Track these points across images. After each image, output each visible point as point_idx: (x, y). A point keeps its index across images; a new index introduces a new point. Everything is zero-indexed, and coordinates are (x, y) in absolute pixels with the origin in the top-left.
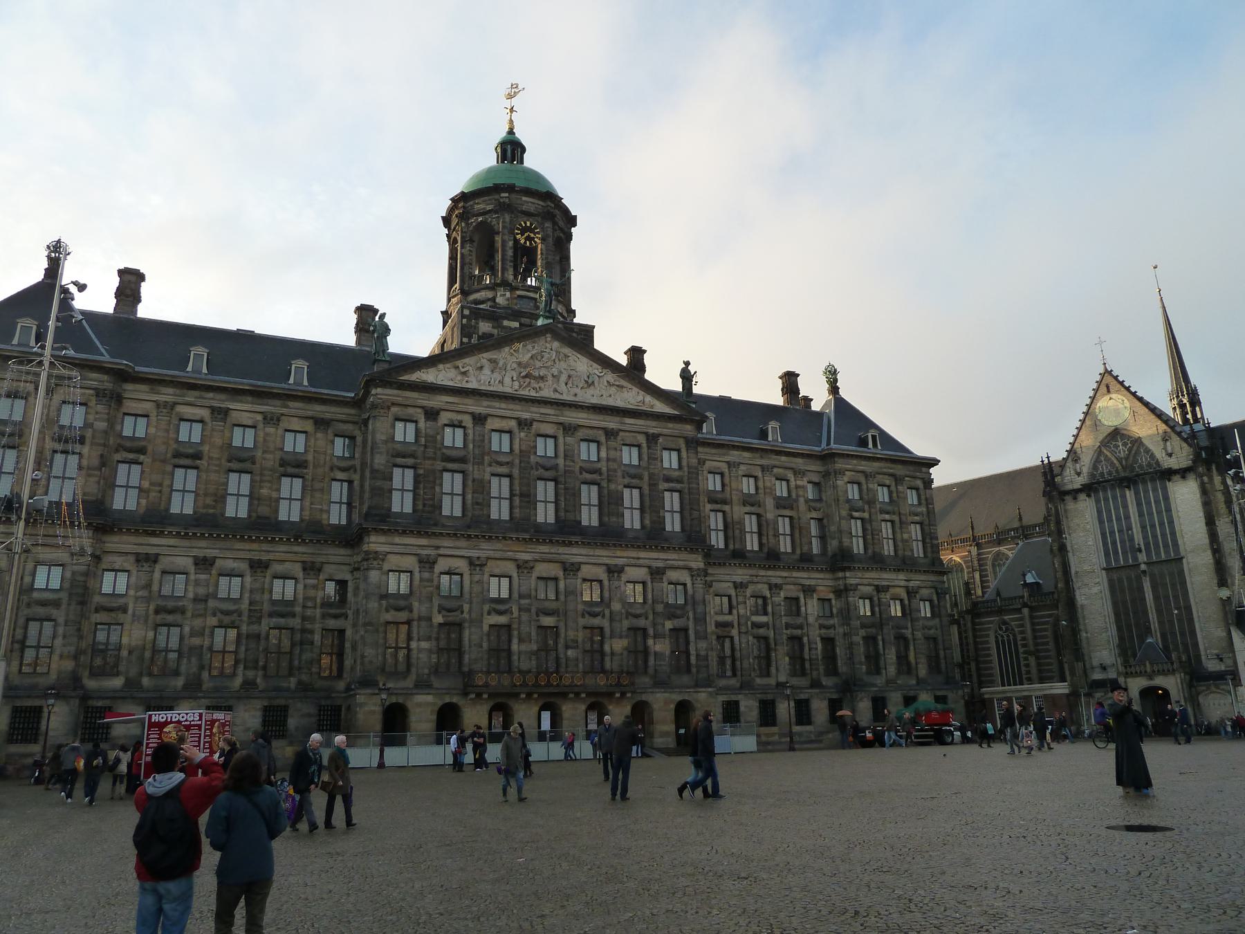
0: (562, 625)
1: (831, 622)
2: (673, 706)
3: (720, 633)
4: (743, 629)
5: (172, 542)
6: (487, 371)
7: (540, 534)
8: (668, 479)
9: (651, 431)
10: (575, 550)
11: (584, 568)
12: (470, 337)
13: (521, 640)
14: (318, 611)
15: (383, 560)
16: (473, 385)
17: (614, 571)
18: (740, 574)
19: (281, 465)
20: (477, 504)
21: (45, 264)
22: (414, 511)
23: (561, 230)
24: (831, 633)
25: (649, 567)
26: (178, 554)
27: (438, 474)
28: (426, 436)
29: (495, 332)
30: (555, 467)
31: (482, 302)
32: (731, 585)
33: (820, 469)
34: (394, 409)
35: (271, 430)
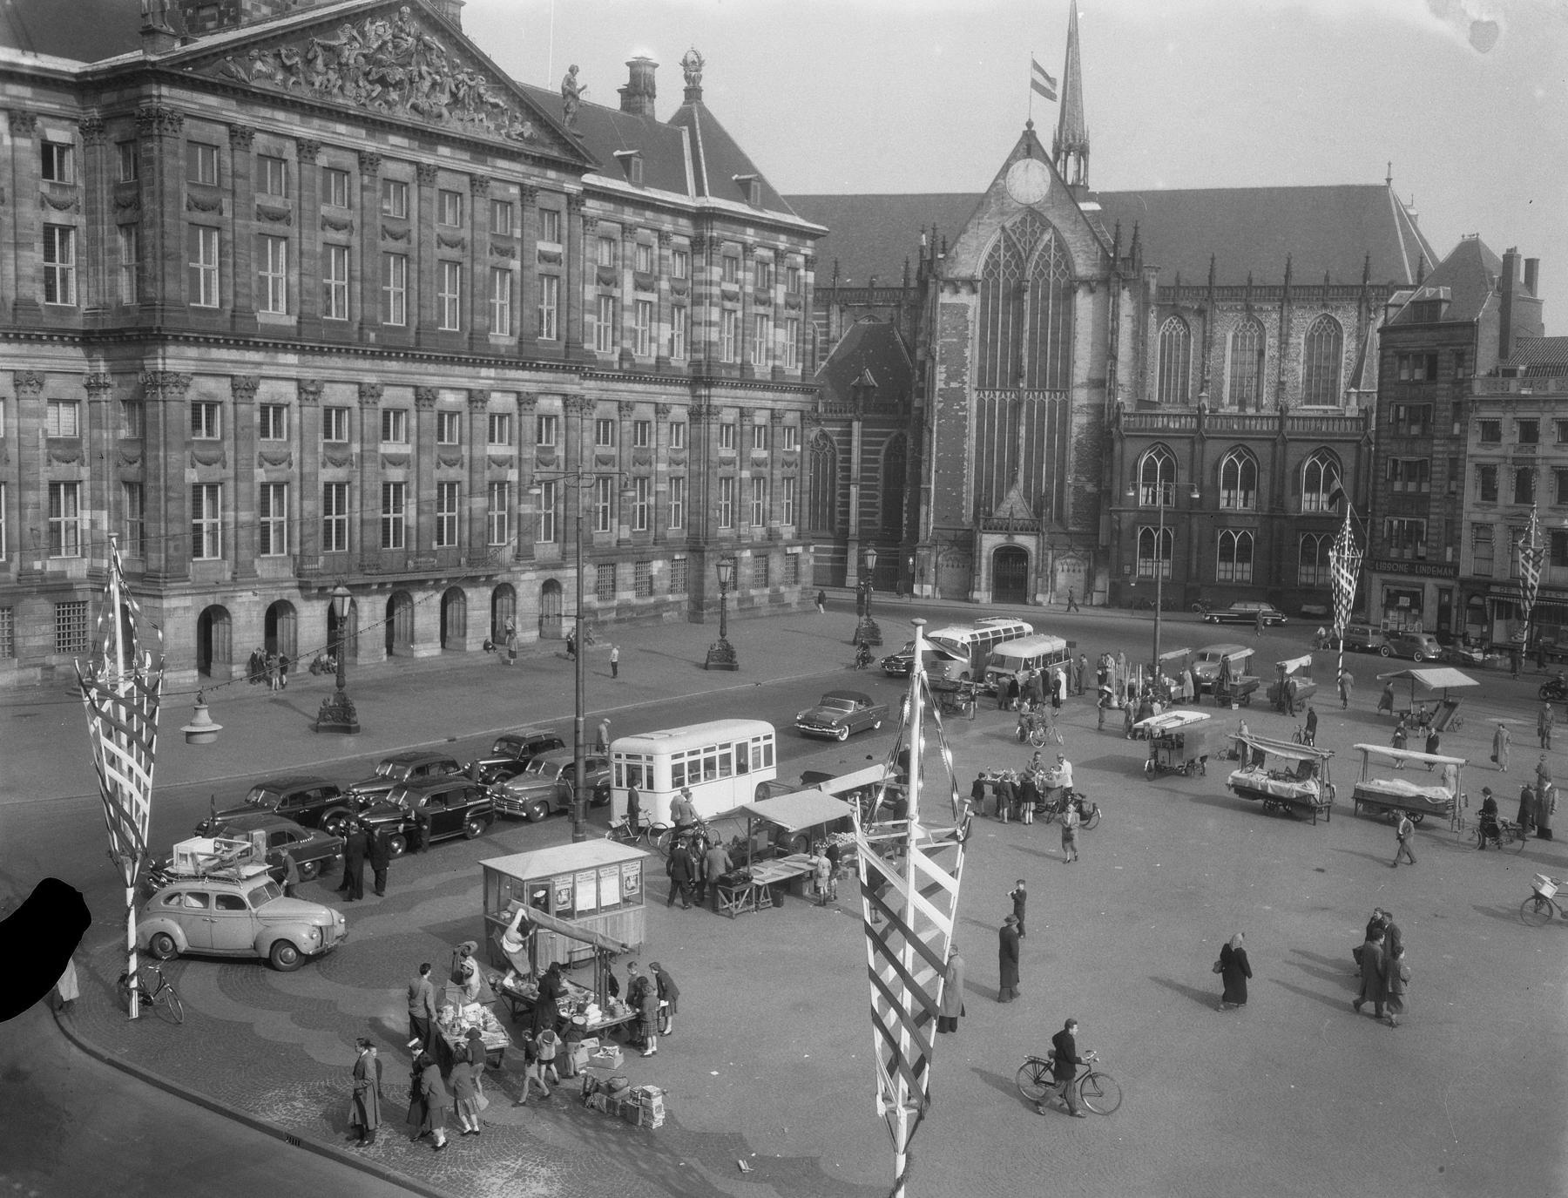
0: (413, 478)
8: (545, 257)
9: (527, 182)
10: (432, 368)
14: (42, 451)
17: (476, 399)
20: (309, 293)
22: (222, 302)
24: (681, 470)
25: (518, 393)
28: (234, 175)
30: (406, 235)
33: (690, 231)
34: (187, 122)
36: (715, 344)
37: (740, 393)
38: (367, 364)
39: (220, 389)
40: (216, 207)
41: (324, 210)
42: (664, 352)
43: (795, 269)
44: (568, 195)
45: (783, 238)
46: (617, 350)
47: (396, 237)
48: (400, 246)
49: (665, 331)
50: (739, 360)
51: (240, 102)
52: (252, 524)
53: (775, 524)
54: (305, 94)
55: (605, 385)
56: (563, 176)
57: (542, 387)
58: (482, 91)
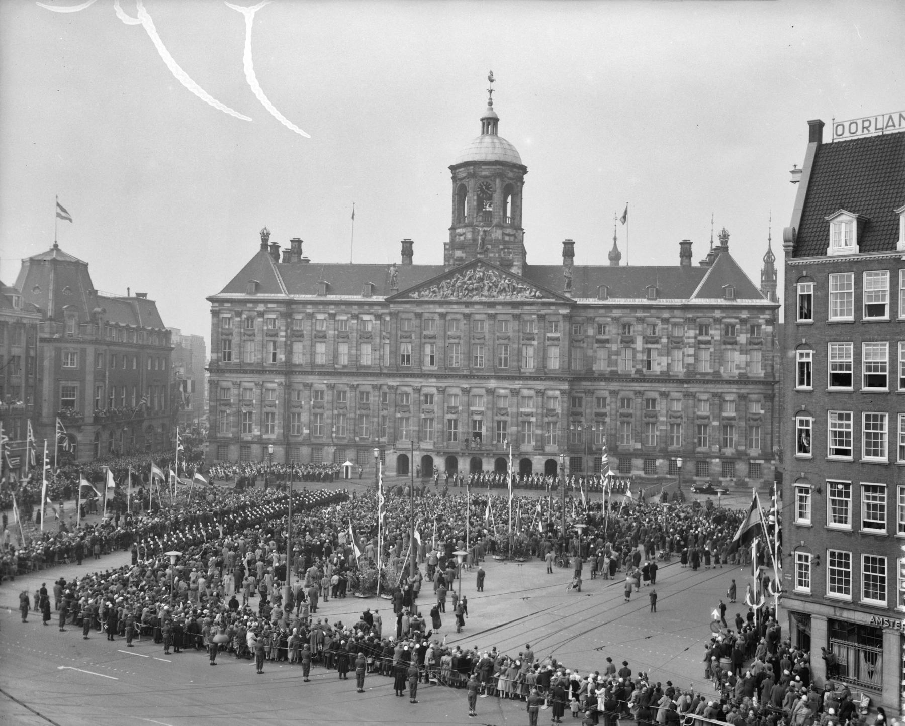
1: (679, 414)
2: (543, 462)
4: (614, 417)
5: (317, 377)
6: (445, 289)
11: (497, 390)
12: (449, 261)
13: (463, 427)
16: (438, 299)
17: (515, 393)
18: (614, 386)
21: (261, 242)
23: (510, 179)
24: (679, 421)
26: (320, 383)
29: (464, 255)
30: (484, 338)
31: (461, 235)
32: (607, 392)
36: (694, 365)
37: (710, 386)
38: (464, 381)
39: (409, 390)
40: (410, 337)
42: (665, 369)
43: (759, 326)
44: (564, 316)
45: (746, 312)
46: (634, 370)
48: (482, 341)
49: (664, 361)
50: (712, 371)
52: (419, 431)
53: (743, 448)
55: (625, 384)
56: (558, 308)
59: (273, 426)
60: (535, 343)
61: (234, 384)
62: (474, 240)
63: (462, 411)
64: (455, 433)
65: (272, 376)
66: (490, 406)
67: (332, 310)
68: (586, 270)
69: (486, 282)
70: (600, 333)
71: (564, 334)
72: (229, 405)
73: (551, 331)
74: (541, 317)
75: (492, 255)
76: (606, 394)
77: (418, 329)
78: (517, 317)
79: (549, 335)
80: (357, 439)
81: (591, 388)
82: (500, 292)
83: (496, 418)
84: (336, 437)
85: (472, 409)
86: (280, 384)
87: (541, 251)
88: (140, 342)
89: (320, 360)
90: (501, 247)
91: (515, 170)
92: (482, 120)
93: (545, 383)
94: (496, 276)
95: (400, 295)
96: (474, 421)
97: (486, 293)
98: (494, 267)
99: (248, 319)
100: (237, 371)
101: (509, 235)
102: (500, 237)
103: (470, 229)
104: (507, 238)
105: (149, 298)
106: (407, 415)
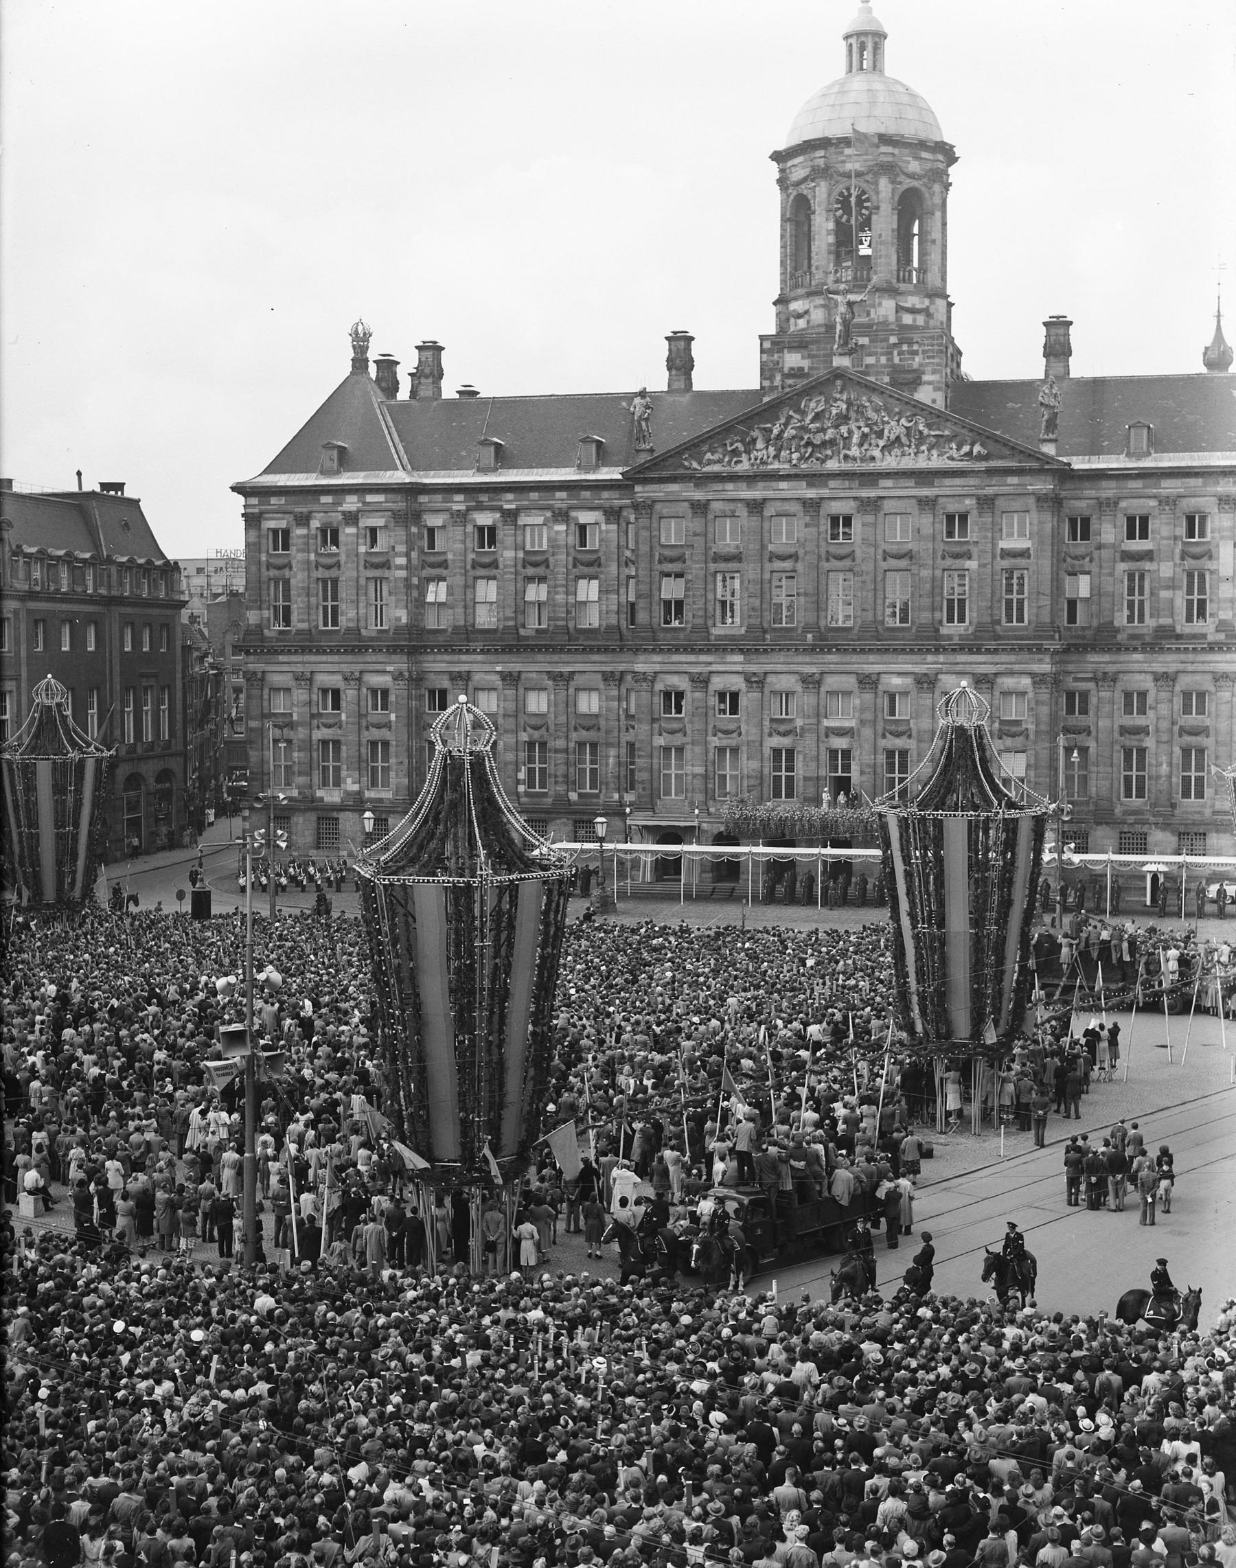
3: (1127, 743)
4: (1165, 738)
5: (480, 657)
6: (760, 444)
7: (827, 641)
8: (1006, 554)
10: (872, 658)
11: (885, 679)
12: (771, 378)
15: (653, 682)
19: (575, 566)
20: (753, 609)
23: (912, 176)
27: (710, 579)
29: (805, 364)
31: (799, 316)
32: (1150, 678)
34: (658, 506)
35: (563, 528)
38: (807, 659)
39: (682, 683)
40: (681, 559)
41: (771, 547)
47: (840, 558)
48: (847, 563)
51: (696, 485)
52: (706, 777)
54: (744, 466)
55: (1191, 657)
56: (1027, 479)
57: (1001, 668)
58: (921, 427)
59: (386, 770)
60: (972, 564)
61: (298, 678)
62: (830, 327)
63: (802, 728)
64: (790, 780)
65: (381, 658)
66: (868, 716)
67: (509, 502)
68: (1097, 385)
69: (853, 426)
70: (1131, 536)
71: (1041, 542)
72: (291, 725)
73: (1010, 535)
74: (986, 503)
75: (870, 360)
76: (1147, 683)
77: (701, 539)
78: (927, 504)
79: (1003, 544)
80: (573, 796)
81: (1111, 669)
82: (887, 448)
83: (883, 743)
84: (527, 794)
85: (826, 723)
86: (398, 676)
87: (993, 348)
88: (103, 591)
89: (485, 618)
90: (893, 340)
91: (924, 155)
92: (847, 37)
93: (997, 658)
94: (877, 411)
95: (657, 463)
96: (833, 753)
97: (854, 451)
98: (872, 389)
99: (323, 531)
100: (304, 650)
101: (912, 311)
102: (892, 318)
103: (819, 301)
104: (907, 319)
105: (129, 493)
106: (678, 740)
